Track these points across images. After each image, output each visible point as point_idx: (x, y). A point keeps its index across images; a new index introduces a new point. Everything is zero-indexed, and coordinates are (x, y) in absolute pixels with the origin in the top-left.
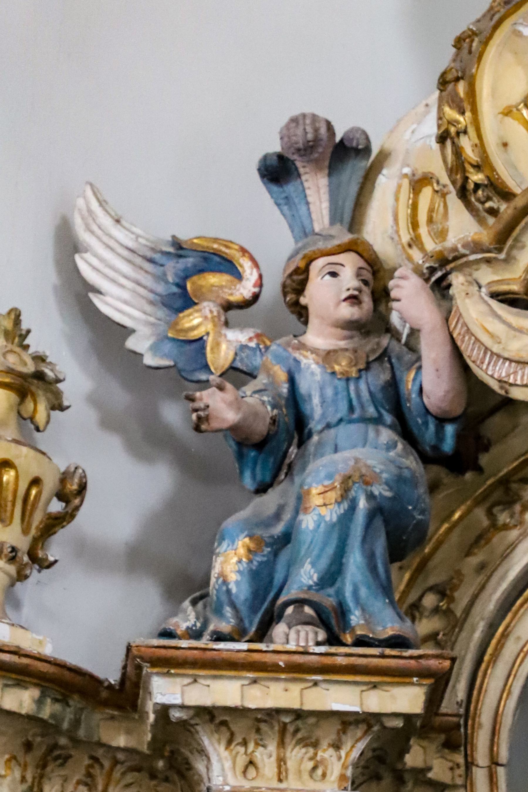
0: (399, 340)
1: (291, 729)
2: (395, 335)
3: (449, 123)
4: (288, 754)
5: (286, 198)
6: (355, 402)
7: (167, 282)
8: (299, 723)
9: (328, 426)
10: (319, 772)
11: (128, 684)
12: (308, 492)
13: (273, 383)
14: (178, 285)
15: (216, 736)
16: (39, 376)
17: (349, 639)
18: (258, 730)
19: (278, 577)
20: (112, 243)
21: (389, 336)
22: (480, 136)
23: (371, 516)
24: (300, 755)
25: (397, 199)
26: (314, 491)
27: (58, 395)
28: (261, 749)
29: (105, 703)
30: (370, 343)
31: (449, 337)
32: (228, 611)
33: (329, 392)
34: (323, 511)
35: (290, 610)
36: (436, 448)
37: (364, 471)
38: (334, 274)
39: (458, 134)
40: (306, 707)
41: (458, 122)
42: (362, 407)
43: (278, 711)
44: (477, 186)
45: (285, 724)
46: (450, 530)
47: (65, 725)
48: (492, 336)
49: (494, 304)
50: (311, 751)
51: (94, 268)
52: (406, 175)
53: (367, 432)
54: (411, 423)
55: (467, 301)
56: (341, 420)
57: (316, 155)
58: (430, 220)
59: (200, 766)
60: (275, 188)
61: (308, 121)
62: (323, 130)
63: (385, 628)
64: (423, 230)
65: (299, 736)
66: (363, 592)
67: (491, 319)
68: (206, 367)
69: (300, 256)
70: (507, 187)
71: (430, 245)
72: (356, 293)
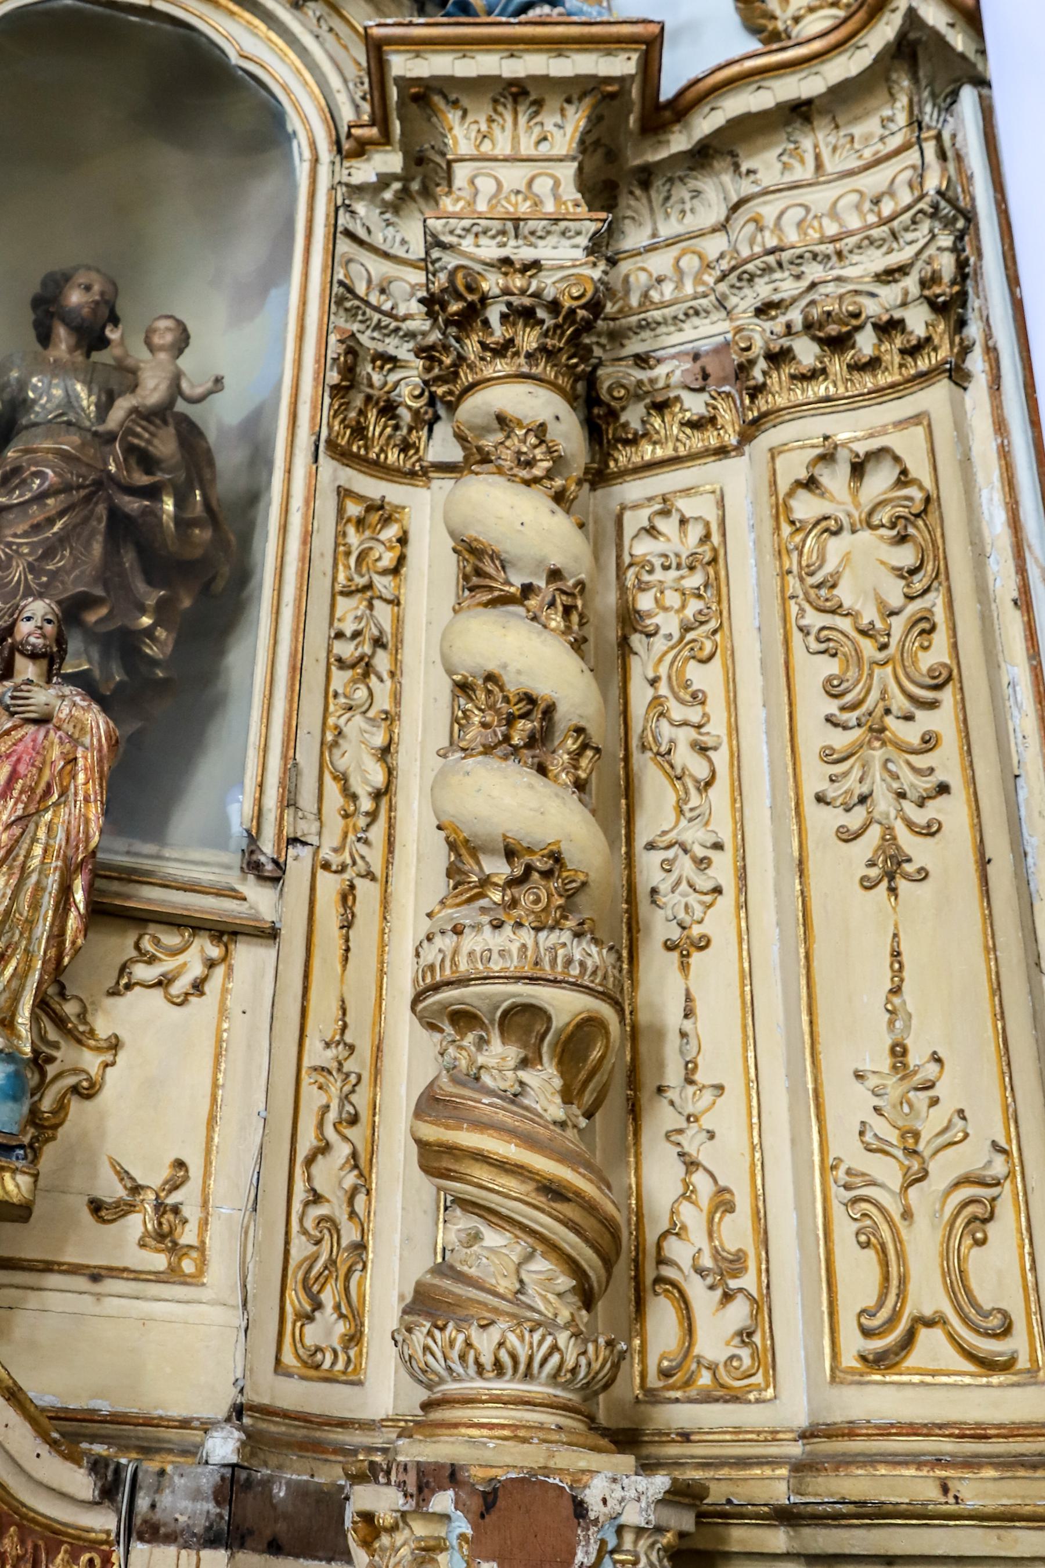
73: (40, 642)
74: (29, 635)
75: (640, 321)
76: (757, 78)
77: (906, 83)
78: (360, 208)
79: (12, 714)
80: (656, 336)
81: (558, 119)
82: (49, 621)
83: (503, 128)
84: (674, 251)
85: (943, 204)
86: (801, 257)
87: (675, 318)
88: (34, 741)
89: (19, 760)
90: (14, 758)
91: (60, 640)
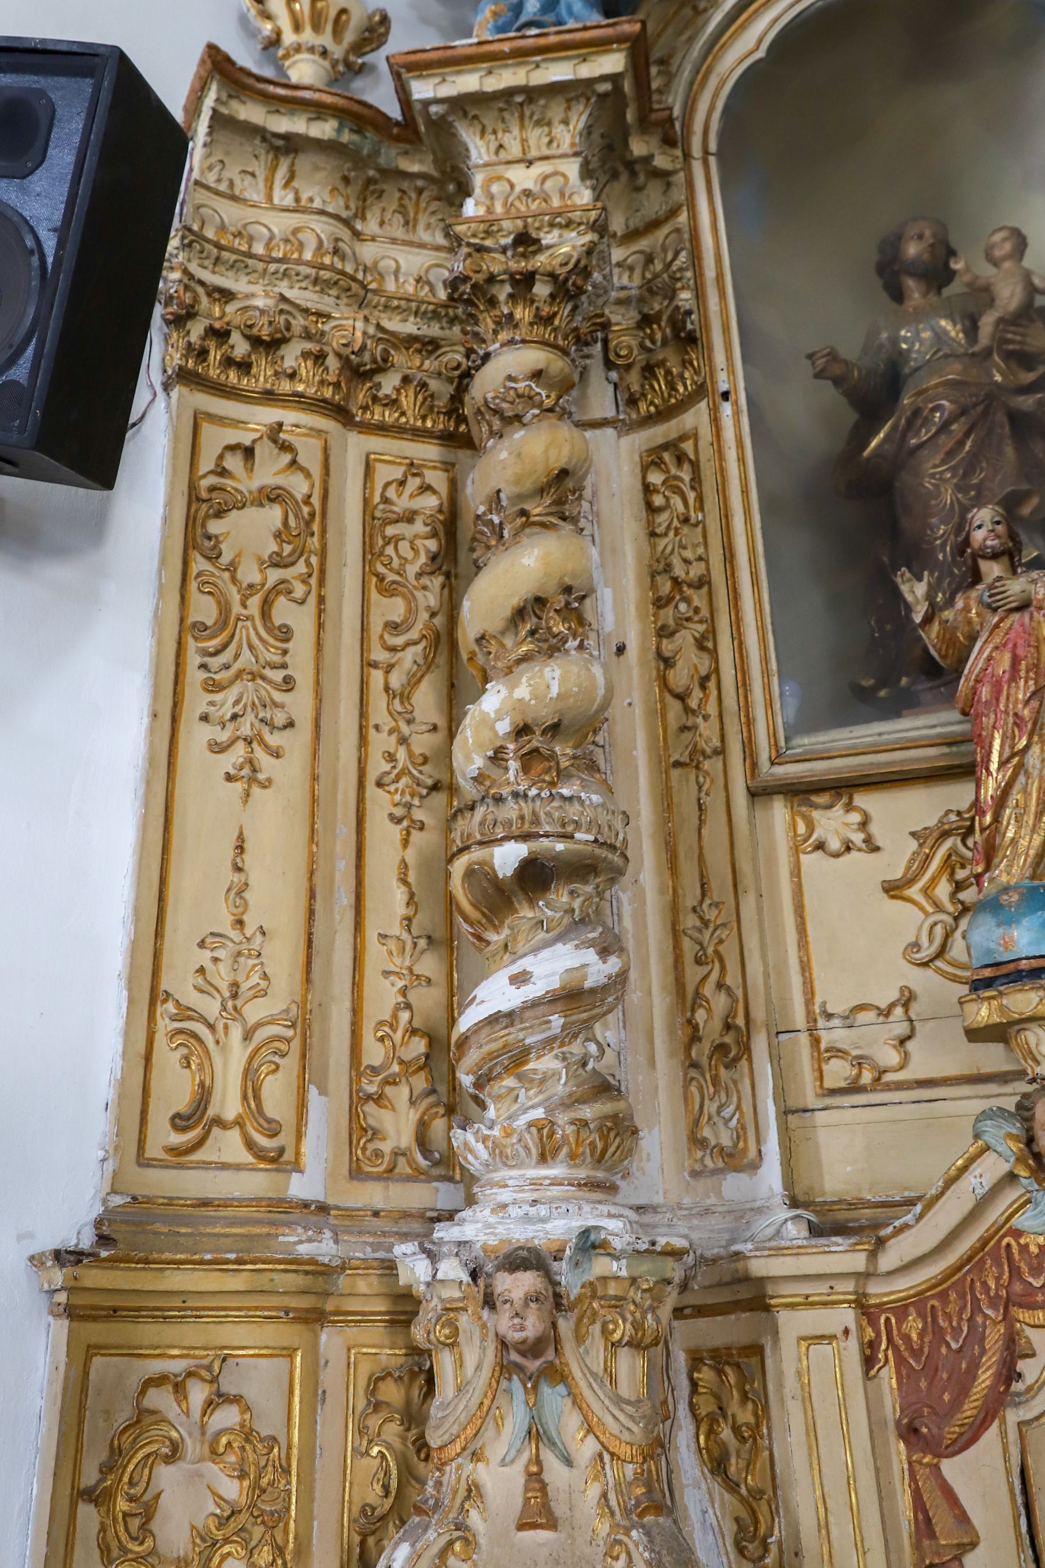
10: (555, 144)
18: (503, 120)
29: (397, 139)
50: (546, 129)
65: (535, 118)
73: (996, 542)
74: (985, 540)
79: (995, 610)
82: (998, 523)
88: (1022, 625)
89: (1015, 646)
90: (1010, 646)
91: (1012, 536)
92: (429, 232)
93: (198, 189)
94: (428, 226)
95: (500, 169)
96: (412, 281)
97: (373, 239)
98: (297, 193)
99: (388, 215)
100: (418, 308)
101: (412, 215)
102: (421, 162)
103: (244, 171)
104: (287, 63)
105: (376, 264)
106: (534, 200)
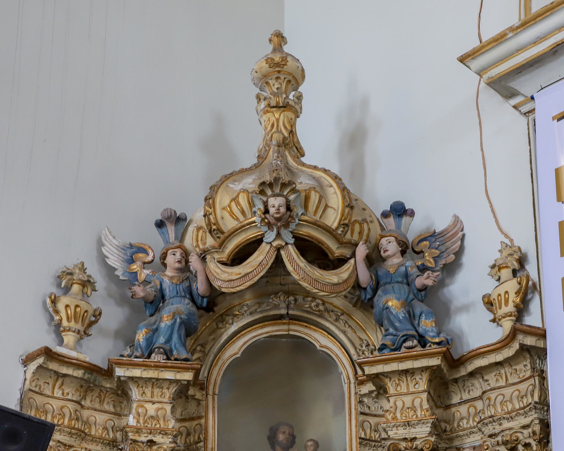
0: (193, 274)
1: (155, 383)
2: (191, 273)
3: (207, 211)
4: (154, 391)
5: (163, 232)
6: (178, 291)
7: (127, 255)
8: (158, 382)
9: (171, 298)
10: (163, 396)
11: (110, 369)
12: (163, 316)
13: (156, 285)
14: (130, 256)
15: (134, 385)
16: (89, 281)
17: (173, 359)
19: (154, 340)
20: (112, 244)
21: (189, 273)
22: (215, 215)
23: (181, 324)
24: (158, 391)
25: (193, 233)
26: (165, 316)
27: (94, 287)
28: (147, 389)
30: (184, 275)
31: (205, 274)
32: (139, 350)
33: (171, 288)
34: (167, 322)
35: (156, 350)
36: (201, 305)
37: (179, 311)
38: (174, 255)
39: (209, 214)
40: (159, 378)
41: (209, 211)
42: (181, 293)
43: (151, 378)
44: (214, 230)
45: (154, 382)
46: (205, 329)
47: (92, 381)
48: (217, 273)
49: (218, 264)
50: (161, 390)
51: (107, 251)
52: (195, 227)
53: (182, 300)
54: (194, 298)
55: (211, 263)
56: (174, 296)
57: (171, 220)
58: (201, 240)
59: (130, 393)
60: (159, 229)
61: (169, 210)
62: (173, 213)
63: (183, 355)
64: (200, 242)
65: (158, 385)
66: (177, 345)
67: (217, 268)
68: (137, 280)
69: (165, 249)
70: (223, 230)
71: (201, 247)
72: (180, 260)
75: (456, 435)
76: (482, 355)
77: (528, 356)
78: (365, 400)
80: (462, 439)
81: (420, 377)
83: (403, 382)
84: (467, 405)
85: (537, 405)
86: (500, 419)
87: (467, 434)
92: (108, 405)
93: (30, 392)
94: (108, 403)
95: (143, 403)
96: (101, 428)
97: (88, 409)
98: (63, 390)
99: (94, 398)
100: (103, 442)
101: (103, 398)
102: (110, 383)
103: (46, 382)
104: (63, 334)
105: (88, 419)
106: (154, 420)
